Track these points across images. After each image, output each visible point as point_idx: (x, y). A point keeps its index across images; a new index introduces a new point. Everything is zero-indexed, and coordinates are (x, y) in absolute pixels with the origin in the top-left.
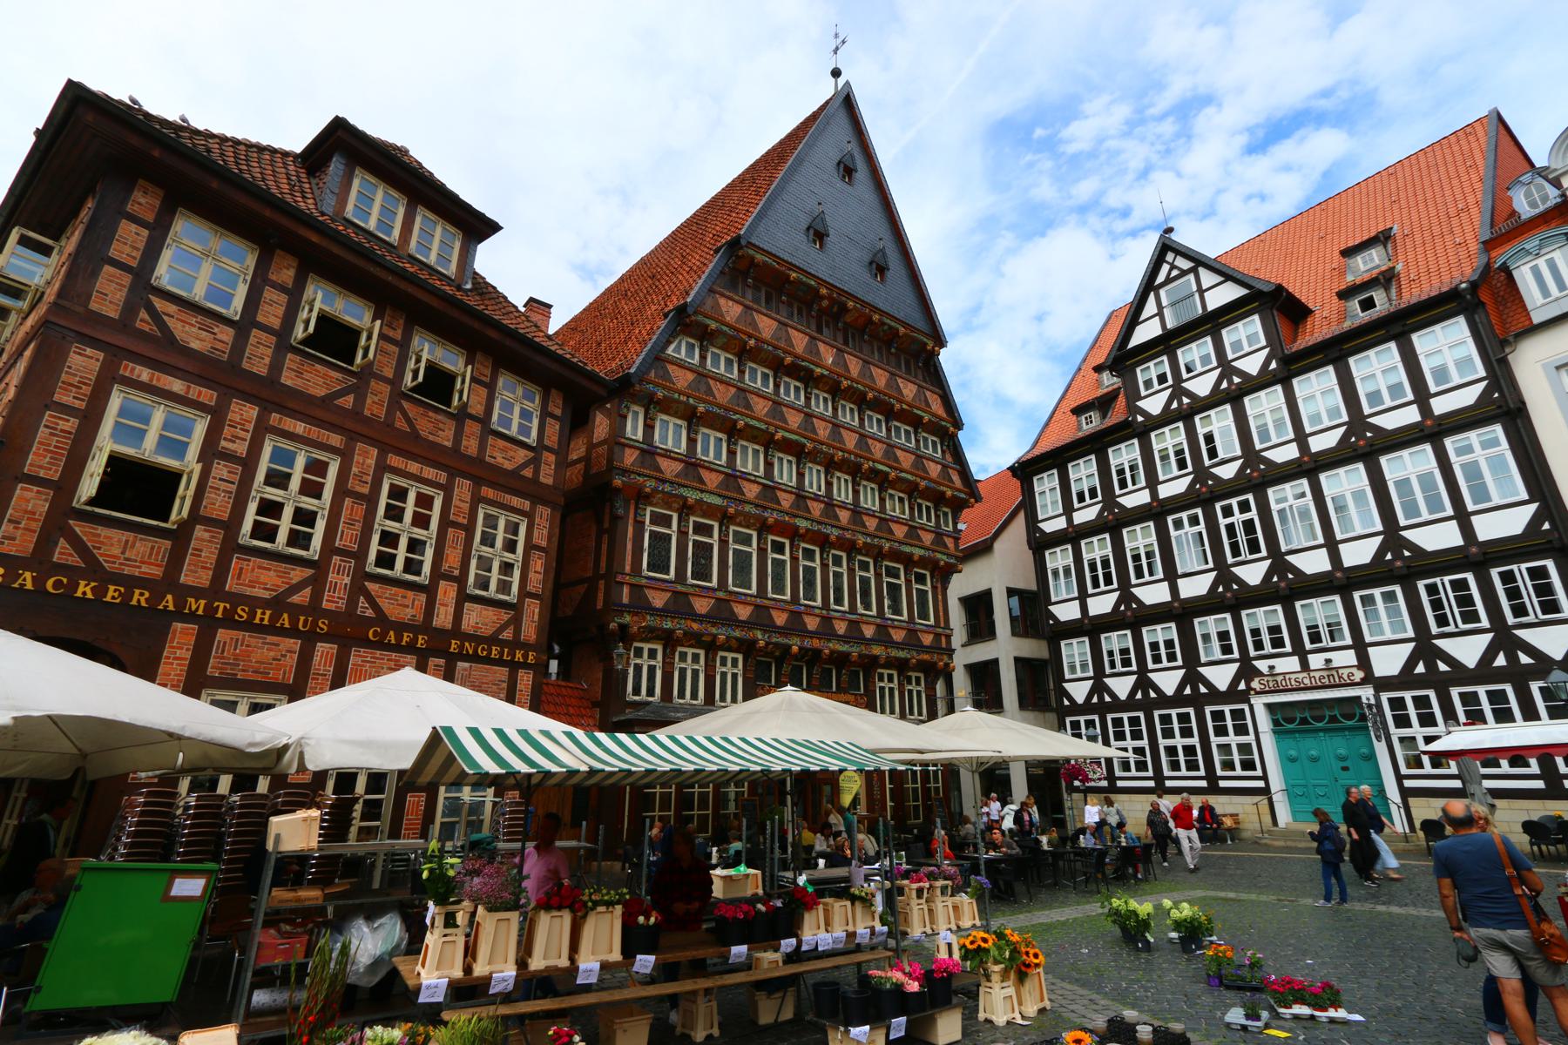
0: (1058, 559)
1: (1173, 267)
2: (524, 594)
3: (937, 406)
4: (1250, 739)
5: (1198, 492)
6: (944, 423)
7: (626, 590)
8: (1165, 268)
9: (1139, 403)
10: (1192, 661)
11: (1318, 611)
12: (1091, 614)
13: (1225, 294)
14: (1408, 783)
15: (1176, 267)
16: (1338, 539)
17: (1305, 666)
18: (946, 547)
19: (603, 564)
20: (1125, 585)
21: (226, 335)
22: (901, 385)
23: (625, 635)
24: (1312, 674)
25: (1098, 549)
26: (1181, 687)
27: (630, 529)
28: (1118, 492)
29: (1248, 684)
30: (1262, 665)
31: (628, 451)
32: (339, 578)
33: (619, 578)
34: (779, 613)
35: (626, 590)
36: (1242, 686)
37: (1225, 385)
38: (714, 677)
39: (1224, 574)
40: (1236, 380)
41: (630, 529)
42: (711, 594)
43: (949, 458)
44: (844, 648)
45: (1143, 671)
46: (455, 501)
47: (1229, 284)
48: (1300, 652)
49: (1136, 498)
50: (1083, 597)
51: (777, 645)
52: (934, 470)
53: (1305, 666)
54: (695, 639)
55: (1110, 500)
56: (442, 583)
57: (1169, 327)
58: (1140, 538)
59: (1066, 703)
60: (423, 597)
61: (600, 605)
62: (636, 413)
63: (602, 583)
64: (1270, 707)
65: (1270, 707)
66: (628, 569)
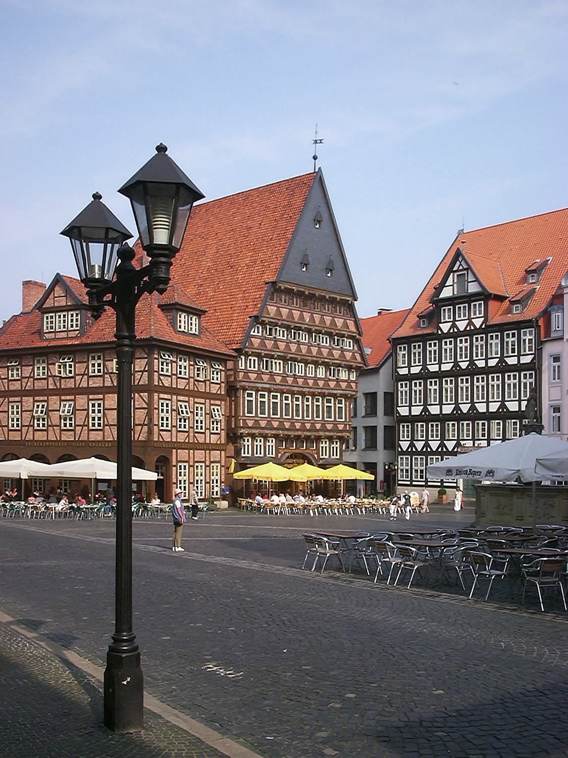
2: (221, 430)
3: (352, 328)
6: (354, 334)
7: (241, 421)
10: (443, 438)
13: (473, 288)
19: (233, 412)
20: (425, 404)
22: (336, 322)
23: (242, 436)
27: (241, 400)
28: (428, 363)
30: (462, 443)
31: (240, 373)
32: (191, 434)
33: (240, 418)
34: (287, 423)
35: (241, 421)
36: (456, 450)
37: (468, 329)
38: (266, 447)
40: (472, 328)
41: (241, 400)
42: (265, 419)
43: (356, 348)
44: (309, 434)
46: (207, 407)
48: (474, 440)
50: (410, 406)
51: (286, 435)
52: (348, 355)
54: (261, 435)
61: (233, 426)
66: (241, 415)
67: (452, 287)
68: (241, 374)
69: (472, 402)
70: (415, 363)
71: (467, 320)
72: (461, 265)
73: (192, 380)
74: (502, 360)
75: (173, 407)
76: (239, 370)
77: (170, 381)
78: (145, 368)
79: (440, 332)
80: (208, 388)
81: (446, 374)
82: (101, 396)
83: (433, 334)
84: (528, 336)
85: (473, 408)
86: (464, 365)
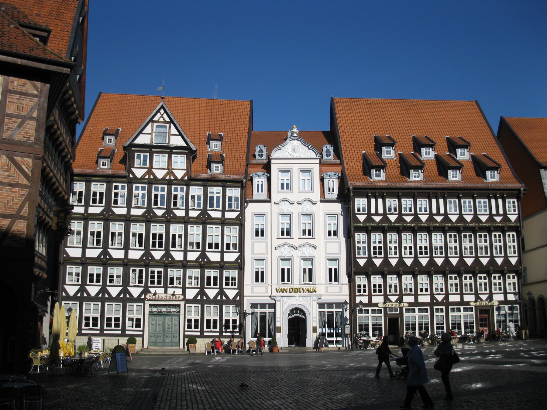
1: (162, 117)
4: (141, 317)
5: (146, 217)
8: (159, 115)
9: (132, 169)
11: (175, 273)
13: (177, 141)
14: (186, 333)
15: (163, 117)
16: (188, 250)
17: (166, 292)
24: (168, 295)
25: (96, 227)
29: (145, 296)
30: (152, 290)
36: (143, 297)
37: (168, 178)
39: (147, 253)
40: (172, 178)
45: (104, 286)
47: (180, 137)
48: (166, 287)
53: (166, 292)
58: (117, 227)
64: (150, 305)
65: (150, 305)
67: (150, 136)
69: (167, 250)
71: (167, 169)
74: (204, 212)
78: (31, 111)
79: (131, 176)
81: (137, 219)
83: (125, 177)
84: (234, 192)
85: (167, 254)
86: (159, 212)
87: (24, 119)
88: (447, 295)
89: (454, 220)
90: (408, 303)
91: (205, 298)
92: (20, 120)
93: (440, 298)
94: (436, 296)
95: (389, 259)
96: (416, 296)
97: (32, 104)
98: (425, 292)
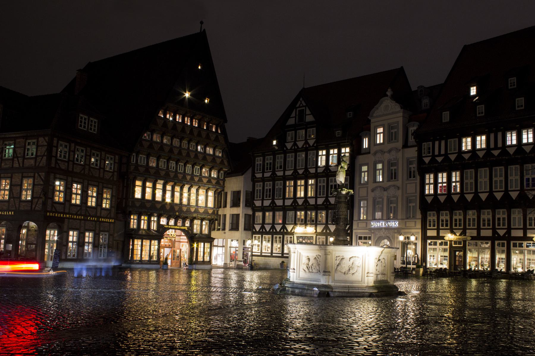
0: (259, 186)
1: (301, 103)
12: (264, 205)
18: (220, 184)
20: (273, 199)
21: (66, 164)
25: (269, 185)
26: (281, 230)
36: (293, 231)
49: (280, 174)
50: (263, 200)
55: (274, 173)
56: (98, 207)
57: (297, 122)
59: (254, 231)
60: (95, 210)
61: (124, 205)
62: (134, 156)
63: (124, 200)
66: (131, 197)
67: (294, 118)
68: (132, 168)
70: (267, 169)
72: (301, 103)
73: (87, 167)
75: (68, 186)
76: (130, 164)
77: (66, 165)
80: (102, 175)
82: (10, 175)
87: (43, 156)
88: (509, 230)
89: (511, 153)
90: (471, 236)
91: (328, 231)
92: (41, 157)
93: (502, 232)
94: (498, 231)
95: (465, 195)
96: (479, 230)
97: (45, 149)
98: (488, 226)
